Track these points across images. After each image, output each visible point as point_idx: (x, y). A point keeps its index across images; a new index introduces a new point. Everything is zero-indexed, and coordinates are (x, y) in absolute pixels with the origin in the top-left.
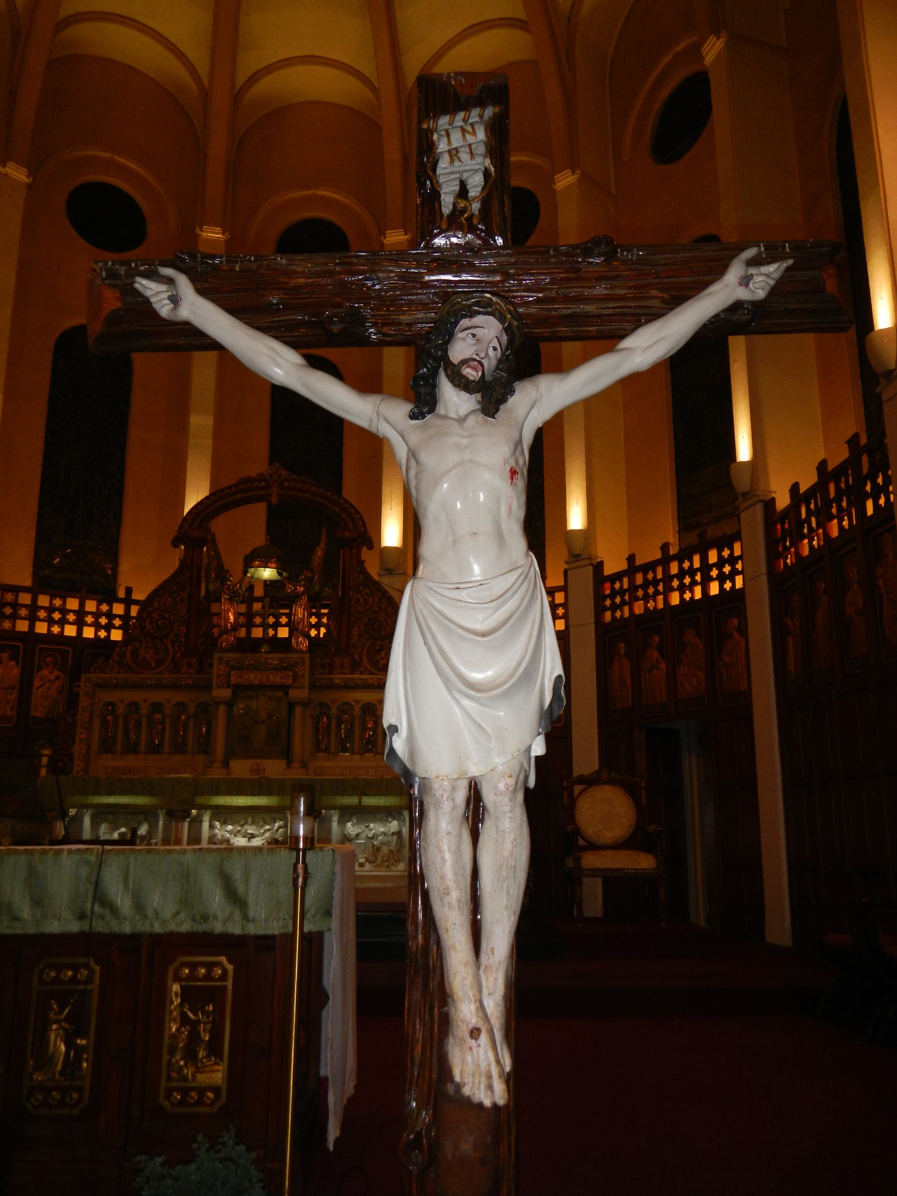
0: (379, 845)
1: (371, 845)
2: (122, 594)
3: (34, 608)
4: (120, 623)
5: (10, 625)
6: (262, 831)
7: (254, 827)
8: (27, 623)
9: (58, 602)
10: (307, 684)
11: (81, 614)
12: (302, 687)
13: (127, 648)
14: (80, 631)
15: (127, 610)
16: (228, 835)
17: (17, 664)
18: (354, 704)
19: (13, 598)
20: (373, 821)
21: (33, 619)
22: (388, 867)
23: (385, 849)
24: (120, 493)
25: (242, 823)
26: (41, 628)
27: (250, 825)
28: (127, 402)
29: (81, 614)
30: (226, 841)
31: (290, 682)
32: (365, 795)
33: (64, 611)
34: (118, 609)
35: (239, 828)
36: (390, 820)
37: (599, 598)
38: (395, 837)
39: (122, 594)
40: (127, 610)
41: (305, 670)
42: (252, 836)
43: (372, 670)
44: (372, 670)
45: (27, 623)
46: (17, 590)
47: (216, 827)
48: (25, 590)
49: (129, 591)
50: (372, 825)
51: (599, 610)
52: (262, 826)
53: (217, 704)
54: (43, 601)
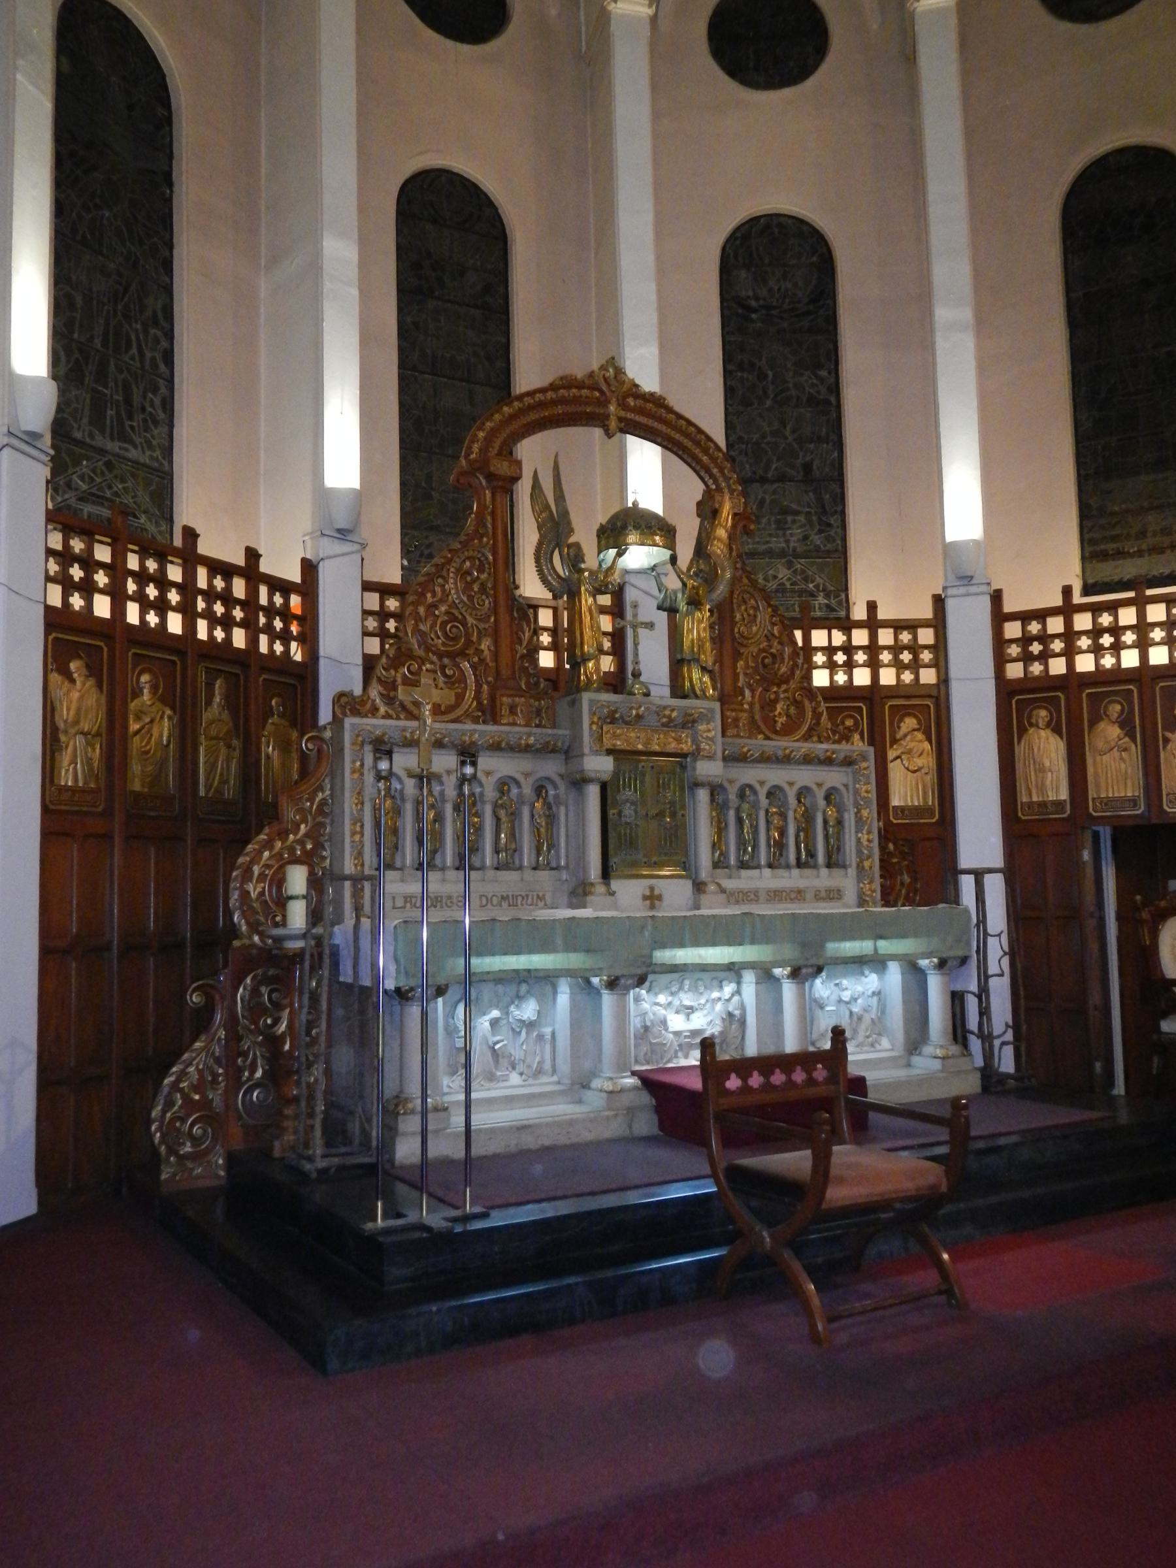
0: (861, 1013)
1: (848, 1013)
6: (703, 1001)
7: (690, 995)
10: (719, 755)
12: (711, 757)
13: (396, 671)
16: (663, 1012)
17: (100, 686)
18: (814, 787)
20: (845, 976)
22: (872, 1045)
23: (867, 1019)
24: (169, 357)
25: (674, 989)
27: (686, 992)
28: (168, 179)
30: (661, 1022)
31: (686, 747)
32: (881, 937)
35: (670, 999)
36: (867, 972)
37: (1000, 643)
38: (875, 999)
41: (711, 730)
42: (690, 1010)
43: (767, 733)
44: (767, 733)
47: (644, 1000)
50: (845, 982)
51: (1000, 661)
52: (701, 994)
53: (696, 785)
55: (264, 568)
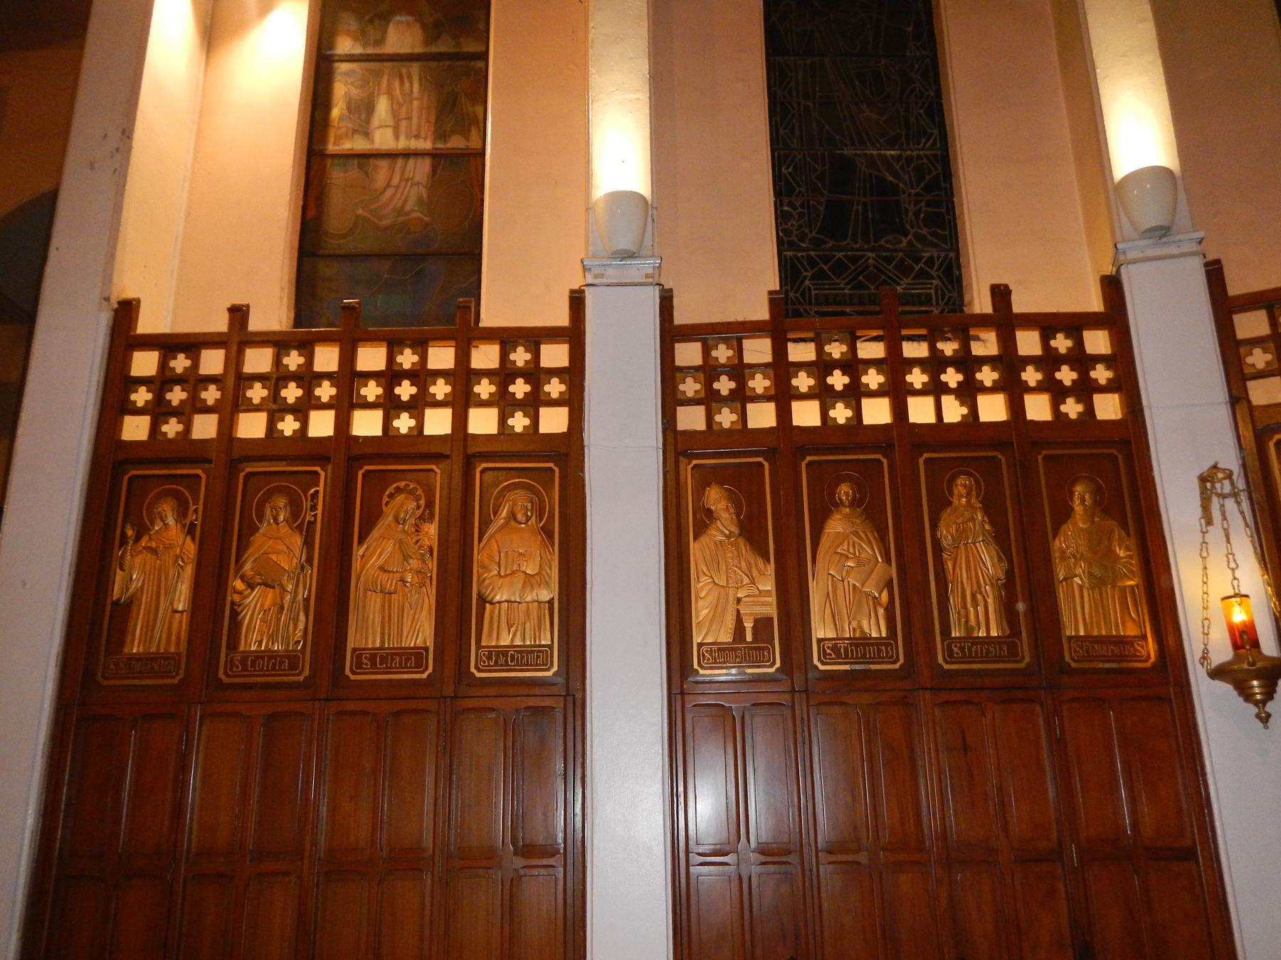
2: (982, 304)
3: (781, 369)
4: (995, 376)
5: (734, 417)
8: (770, 408)
9: (836, 350)
11: (895, 366)
14: (900, 410)
15: (1007, 342)
19: (730, 353)
21: (783, 397)
26: (806, 414)
29: (895, 366)
33: (853, 366)
34: (986, 344)
39: (982, 304)
40: (1007, 342)
45: (770, 408)
46: (735, 332)
48: (753, 329)
49: (1001, 294)
54: (801, 352)
55: (1020, 304)
